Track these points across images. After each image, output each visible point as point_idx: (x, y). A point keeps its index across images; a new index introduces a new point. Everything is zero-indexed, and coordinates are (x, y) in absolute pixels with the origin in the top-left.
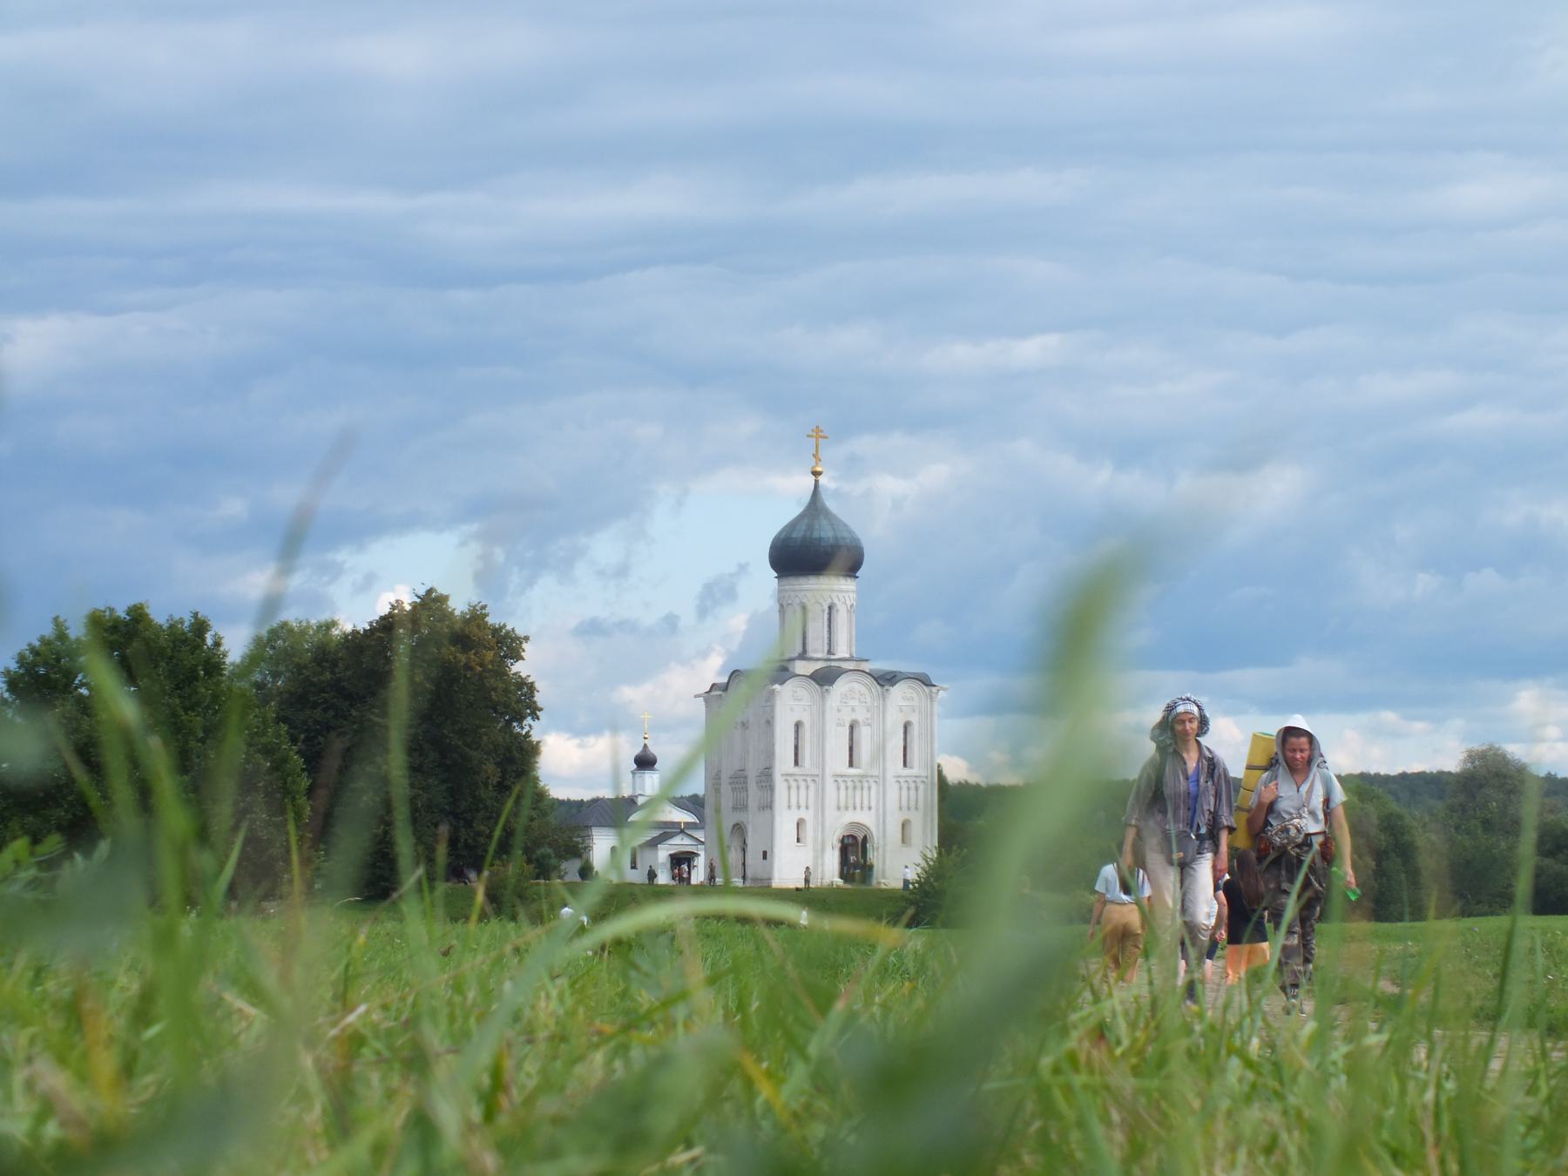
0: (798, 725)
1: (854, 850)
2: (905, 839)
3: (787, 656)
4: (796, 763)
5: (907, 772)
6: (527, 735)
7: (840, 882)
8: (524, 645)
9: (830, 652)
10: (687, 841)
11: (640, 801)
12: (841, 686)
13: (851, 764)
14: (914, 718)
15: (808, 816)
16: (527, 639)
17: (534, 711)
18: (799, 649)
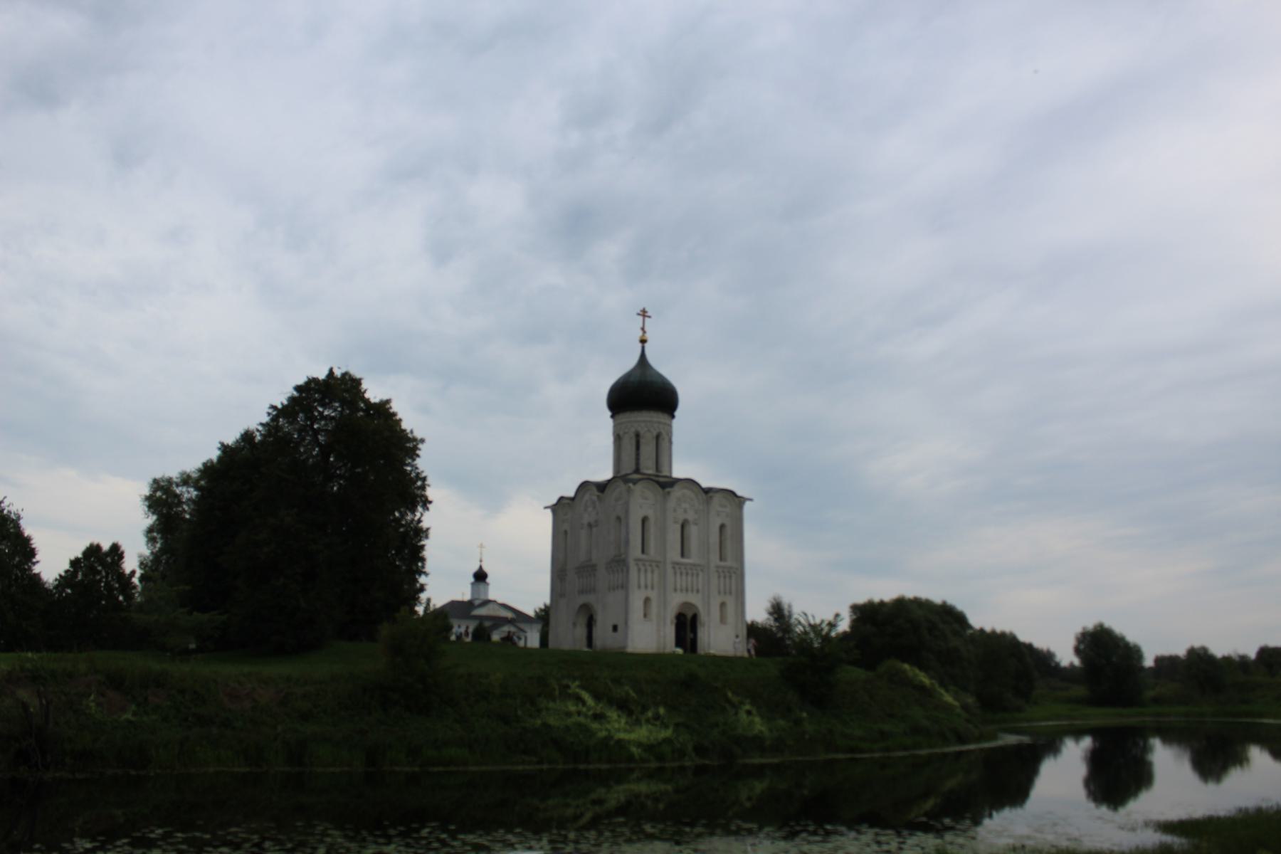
0: (644, 520)
1: (687, 625)
2: (723, 620)
3: (623, 473)
4: (643, 552)
5: (722, 564)
6: (419, 521)
7: (680, 651)
8: (420, 446)
9: (657, 469)
10: (513, 629)
11: (477, 603)
12: (677, 492)
13: (683, 555)
14: (728, 522)
15: (653, 594)
16: (422, 441)
17: (426, 503)
18: (633, 467)
